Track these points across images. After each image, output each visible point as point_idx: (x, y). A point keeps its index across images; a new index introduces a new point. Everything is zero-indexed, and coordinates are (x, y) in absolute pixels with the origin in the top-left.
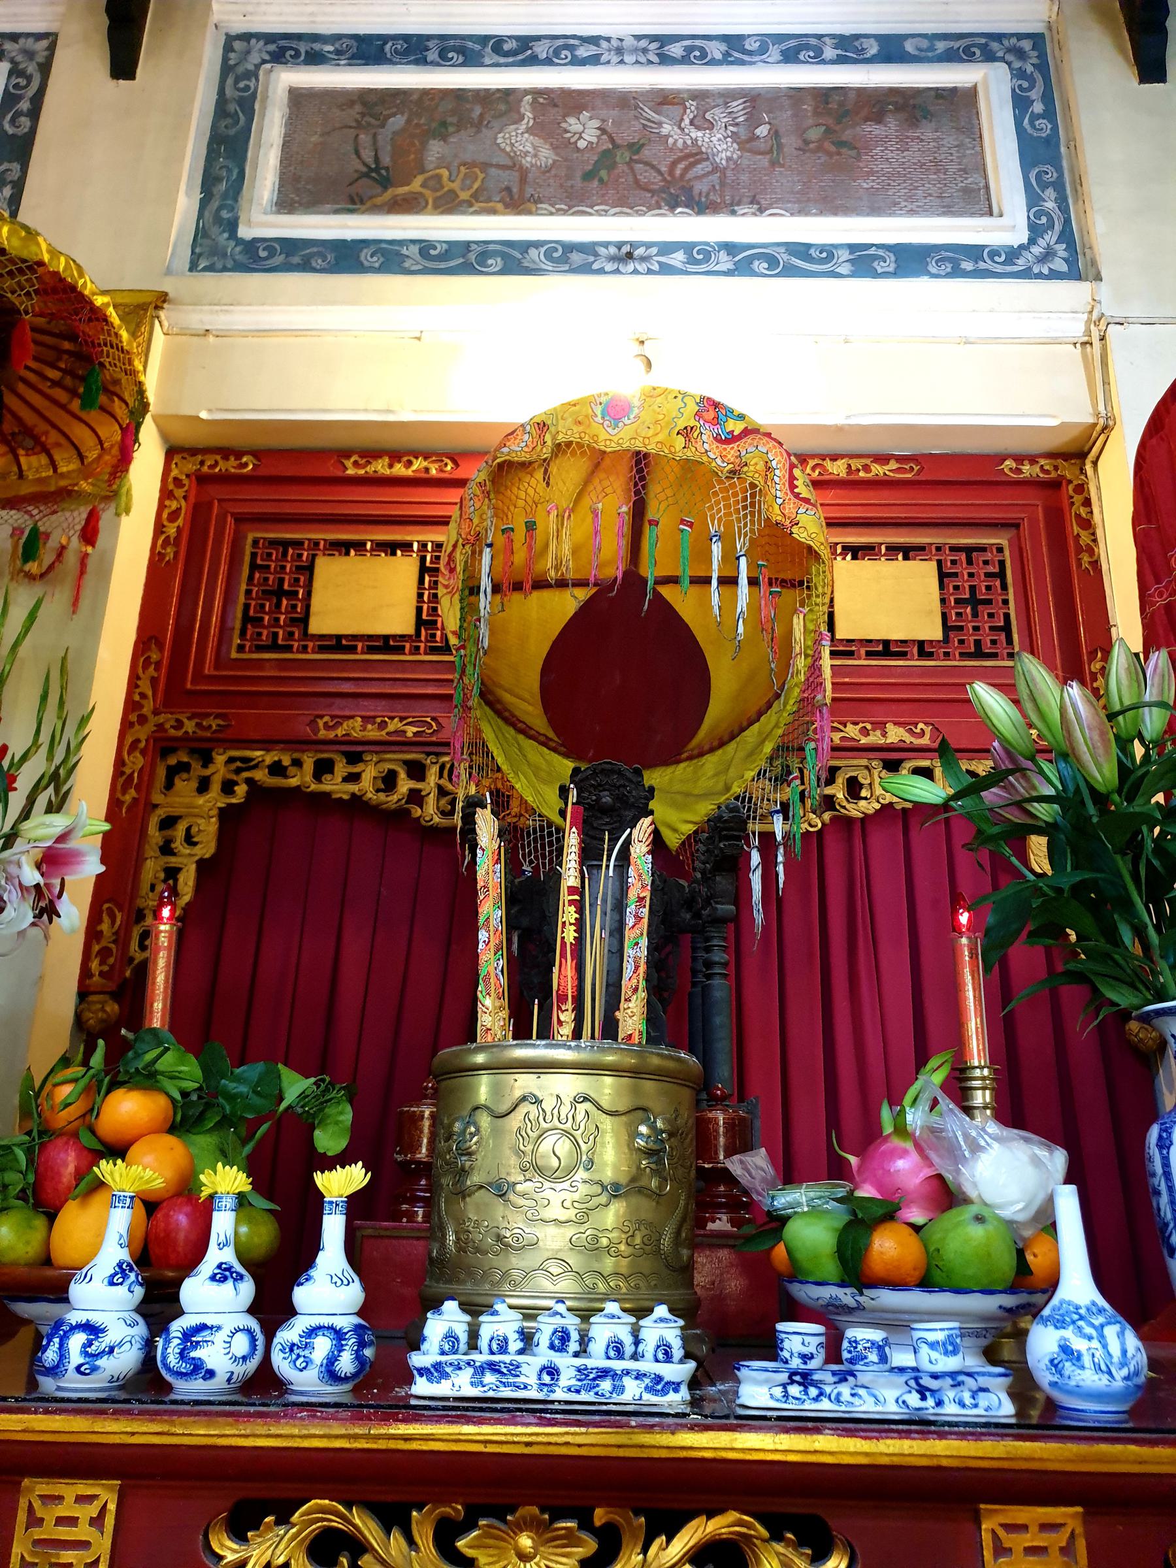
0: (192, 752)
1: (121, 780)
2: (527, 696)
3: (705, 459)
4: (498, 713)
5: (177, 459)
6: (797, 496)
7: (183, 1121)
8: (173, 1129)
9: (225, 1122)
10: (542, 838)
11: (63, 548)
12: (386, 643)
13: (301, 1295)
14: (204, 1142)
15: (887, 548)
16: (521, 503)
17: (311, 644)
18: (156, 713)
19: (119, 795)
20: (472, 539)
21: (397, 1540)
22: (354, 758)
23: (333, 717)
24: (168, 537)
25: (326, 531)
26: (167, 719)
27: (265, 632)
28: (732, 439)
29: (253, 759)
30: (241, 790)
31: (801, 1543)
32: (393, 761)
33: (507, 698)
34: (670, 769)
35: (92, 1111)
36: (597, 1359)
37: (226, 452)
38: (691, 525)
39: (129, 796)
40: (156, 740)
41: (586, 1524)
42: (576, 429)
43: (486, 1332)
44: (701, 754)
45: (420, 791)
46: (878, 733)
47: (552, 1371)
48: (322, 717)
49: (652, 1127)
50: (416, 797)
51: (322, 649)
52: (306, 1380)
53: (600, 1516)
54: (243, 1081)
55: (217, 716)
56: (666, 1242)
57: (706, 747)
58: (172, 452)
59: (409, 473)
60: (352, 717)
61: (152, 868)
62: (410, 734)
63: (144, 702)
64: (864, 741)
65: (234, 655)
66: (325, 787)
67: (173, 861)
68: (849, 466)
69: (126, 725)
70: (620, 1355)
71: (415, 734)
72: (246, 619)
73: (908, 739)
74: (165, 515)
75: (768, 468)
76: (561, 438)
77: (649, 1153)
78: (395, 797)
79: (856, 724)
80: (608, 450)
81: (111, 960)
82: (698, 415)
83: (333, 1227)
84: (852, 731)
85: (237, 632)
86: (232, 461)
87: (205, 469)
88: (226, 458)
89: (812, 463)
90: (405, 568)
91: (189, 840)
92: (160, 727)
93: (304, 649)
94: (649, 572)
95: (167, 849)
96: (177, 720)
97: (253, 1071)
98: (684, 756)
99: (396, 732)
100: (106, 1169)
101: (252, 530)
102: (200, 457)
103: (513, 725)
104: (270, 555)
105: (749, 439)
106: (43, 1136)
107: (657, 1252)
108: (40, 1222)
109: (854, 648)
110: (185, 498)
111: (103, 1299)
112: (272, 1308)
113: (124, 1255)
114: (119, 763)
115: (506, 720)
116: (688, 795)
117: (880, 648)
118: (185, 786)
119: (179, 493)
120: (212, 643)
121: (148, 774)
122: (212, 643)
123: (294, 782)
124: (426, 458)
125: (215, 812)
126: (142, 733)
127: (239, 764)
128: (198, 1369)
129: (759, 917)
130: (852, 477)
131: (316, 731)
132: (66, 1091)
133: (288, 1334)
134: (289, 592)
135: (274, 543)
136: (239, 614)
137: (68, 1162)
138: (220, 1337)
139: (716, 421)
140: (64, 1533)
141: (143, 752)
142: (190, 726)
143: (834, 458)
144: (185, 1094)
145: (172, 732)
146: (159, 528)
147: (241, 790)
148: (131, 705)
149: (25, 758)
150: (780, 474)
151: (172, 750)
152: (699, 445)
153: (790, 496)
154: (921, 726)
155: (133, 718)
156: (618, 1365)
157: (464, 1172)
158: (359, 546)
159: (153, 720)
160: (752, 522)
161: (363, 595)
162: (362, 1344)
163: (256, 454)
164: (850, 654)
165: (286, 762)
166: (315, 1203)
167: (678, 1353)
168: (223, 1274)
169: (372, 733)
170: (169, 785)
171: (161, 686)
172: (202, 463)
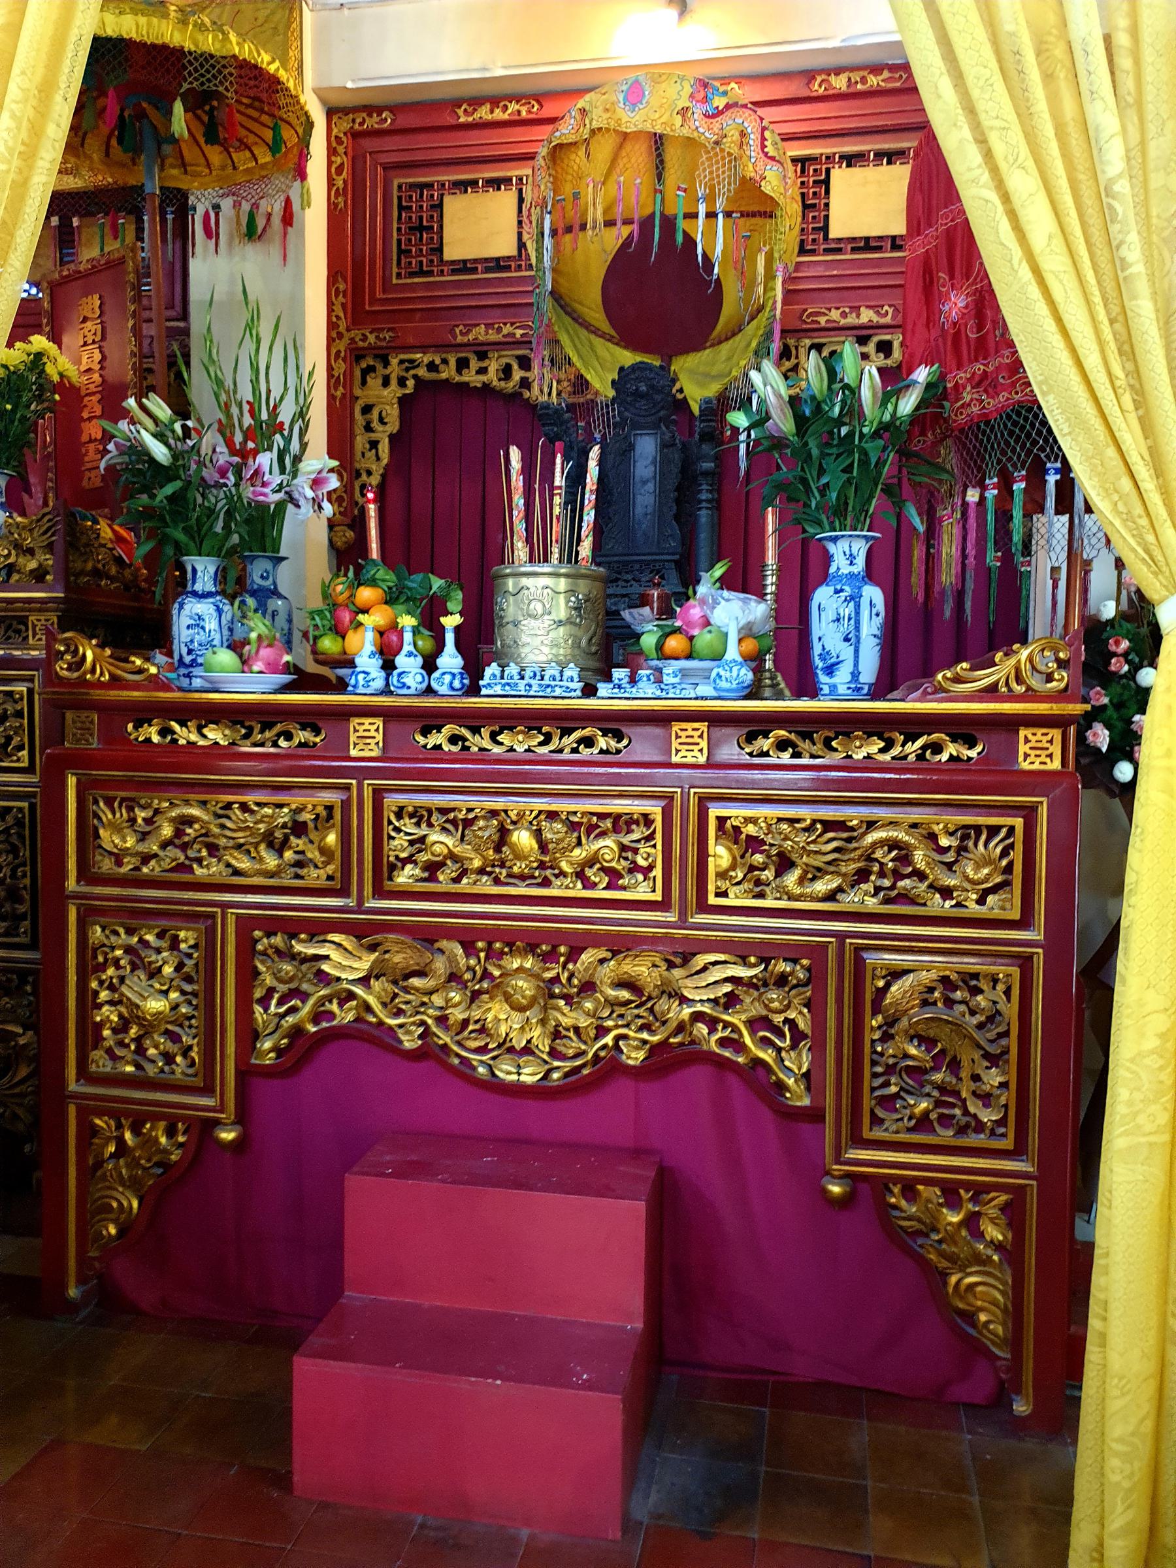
0: (376, 357)
1: (333, 381)
2: (593, 306)
3: (696, 134)
4: (575, 320)
7: (390, 599)
8: (386, 603)
9: (408, 599)
10: (608, 413)
11: (270, 215)
12: (499, 264)
13: (440, 662)
14: (400, 607)
15: (875, 155)
16: (569, 177)
17: (446, 269)
18: (348, 330)
19: (333, 391)
20: (540, 202)
21: (477, 736)
22: (482, 356)
23: (465, 326)
24: (338, 189)
26: (356, 334)
27: (414, 261)
28: (719, 113)
29: (414, 361)
30: (411, 383)
31: (614, 737)
32: (509, 357)
34: (700, 354)
35: (352, 596)
36: (546, 682)
37: (371, 109)
38: (685, 191)
40: (351, 350)
41: (540, 732)
42: (606, 116)
43: (506, 674)
44: (720, 342)
45: (527, 378)
46: (854, 315)
47: (530, 686)
48: (458, 326)
49: (577, 598)
50: (525, 383)
51: (454, 272)
52: (443, 690)
53: (545, 729)
54: (415, 581)
55: (389, 330)
56: (583, 643)
57: (723, 338)
59: (506, 117)
60: (478, 325)
61: (361, 442)
62: (518, 336)
63: (340, 323)
64: (843, 322)
65: (395, 281)
66: (465, 379)
67: (373, 436)
68: (850, 79)
70: (554, 680)
71: (522, 335)
72: (400, 252)
73: (875, 319)
74: (333, 170)
75: (743, 134)
76: (595, 125)
77: (575, 609)
78: (511, 384)
79: (837, 308)
80: (629, 131)
81: (344, 504)
82: (692, 96)
83: (450, 638)
84: (835, 315)
85: (395, 262)
87: (357, 126)
89: (819, 79)
90: (506, 199)
91: (382, 421)
92: (352, 339)
93: (442, 273)
95: (368, 428)
96: (363, 335)
97: (418, 577)
98: (708, 344)
99: (508, 335)
100: (361, 617)
101: (398, 176)
102: (351, 116)
103: (587, 328)
104: (411, 197)
106: (334, 607)
108: (340, 639)
109: (842, 245)
110: (345, 153)
111: (368, 662)
112: (429, 666)
113: (373, 649)
114: (330, 369)
115: (581, 324)
117: (862, 244)
118: (374, 382)
119: (341, 149)
120: (379, 273)
121: (349, 374)
122: (379, 273)
123: (444, 376)
124: (518, 102)
125: (395, 400)
126: (341, 345)
127: (407, 364)
128: (404, 685)
129: (743, 465)
130: (851, 90)
131: (455, 337)
132: (340, 588)
133: (436, 675)
134: (426, 228)
135: (412, 186)
137: (346, 617)
138: (411, 675)
139: (705, 100)
140: (366, 734)
141: (344, 360)
143: (838, 71)
144: (390, 588)
145: (361, 344)
146: (331, 182)
147: (411, 383)
148: (331, 326)
150: (754, 139)
151: (363, 357)
152: (691, 124)
153: (761, 155)
154: (886, 308)
155: (334, 335)
156: (553, 683)
157: (502, 617)
158: (473, 183)
159: (347, 336)
160: (729, 184)
161: (479, 226)
162: (462, 678)
163: (394, 109)
164: (839, 251)
165: (438, 361)
166: (442, 630)
167: (576, 679)
168: (410, 654)
169: (493, 336)
170: (364, 383)
171: (349, 311)
172: (354, 121)
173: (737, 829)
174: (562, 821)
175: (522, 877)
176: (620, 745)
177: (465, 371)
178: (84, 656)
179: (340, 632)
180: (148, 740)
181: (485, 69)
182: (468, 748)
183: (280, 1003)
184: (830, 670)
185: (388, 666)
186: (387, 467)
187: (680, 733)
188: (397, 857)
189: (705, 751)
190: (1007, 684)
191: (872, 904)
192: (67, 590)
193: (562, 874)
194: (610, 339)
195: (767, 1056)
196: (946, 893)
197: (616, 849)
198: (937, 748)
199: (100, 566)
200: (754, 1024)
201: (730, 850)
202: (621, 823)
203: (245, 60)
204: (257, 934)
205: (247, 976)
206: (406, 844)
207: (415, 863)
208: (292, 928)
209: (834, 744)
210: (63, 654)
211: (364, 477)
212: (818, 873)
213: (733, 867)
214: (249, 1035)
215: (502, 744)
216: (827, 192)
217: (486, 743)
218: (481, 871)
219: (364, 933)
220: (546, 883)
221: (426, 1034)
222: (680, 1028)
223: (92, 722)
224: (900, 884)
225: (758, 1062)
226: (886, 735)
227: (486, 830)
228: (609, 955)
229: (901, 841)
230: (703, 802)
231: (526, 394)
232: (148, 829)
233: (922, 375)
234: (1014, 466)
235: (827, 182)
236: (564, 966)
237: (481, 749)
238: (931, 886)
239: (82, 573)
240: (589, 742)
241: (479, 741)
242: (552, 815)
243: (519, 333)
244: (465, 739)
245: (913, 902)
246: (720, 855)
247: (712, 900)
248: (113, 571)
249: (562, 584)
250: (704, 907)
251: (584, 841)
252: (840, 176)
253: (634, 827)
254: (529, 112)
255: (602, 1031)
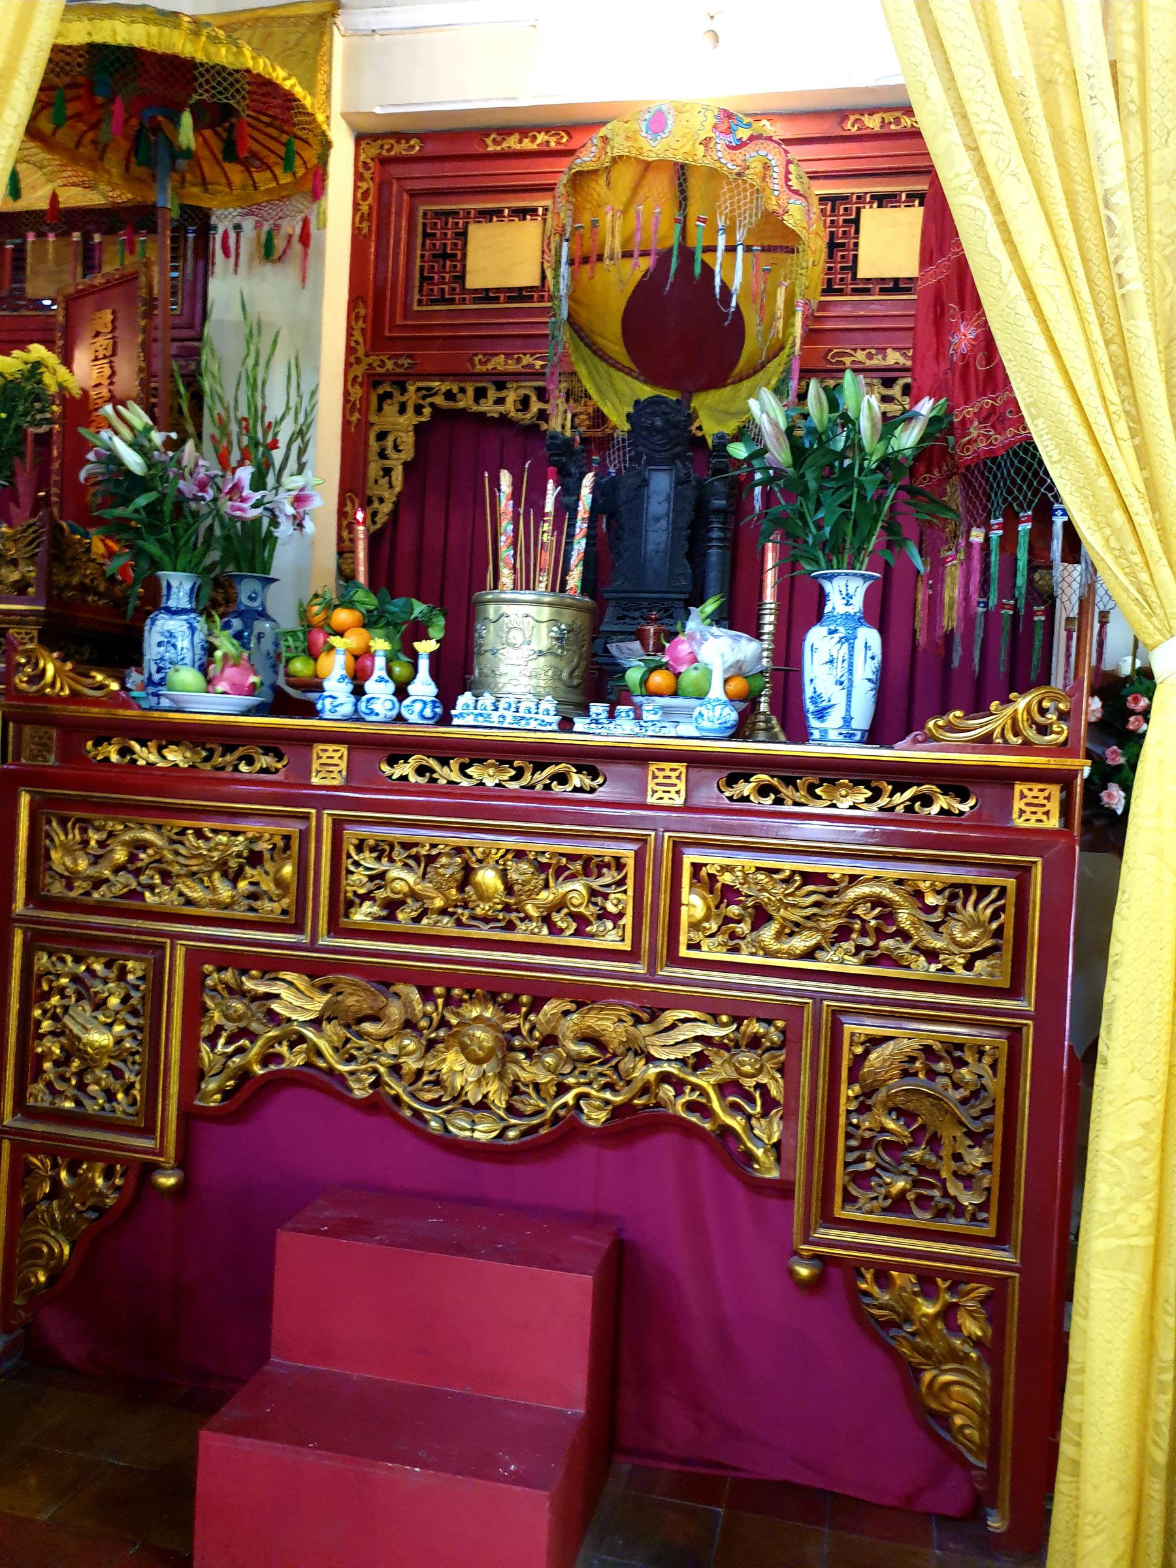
0: (394, 383)
4: (595, 352)
5: (363, 144)
6: (789, 187)
7: (369, 622)
8: (364, 626)
9: (388, 624)
11: (291, 236)
12: (520, 294)
13: (411, 689)
15: (908, 196)
18: (367, 355)
22: (501, 386)
25: (477, 202)
26: (374, 359)
28: (741, 145)
29: (431, 389)
30: (427, 411)
32: (527, 388)
33: (600, 340)
35: (328, 618)
36: (521, 714)
37: (399, 136)
39: (355, 417)
41: (512, 767)
44: (741, 380)
50: (543, 415)
51: (475, 301)
52: (413, 718)
53: (516, 763)
54: (396, 606)
55: (409, 356)
56: (564, 675)
58: (361, 138)
59: (534, 147)
61: (374, 469)
64: (869, 363)
65: (416, 308)
66: (483, 409)
67: (387, 463)
69: (348, 365)
72: (423, 279)
75: (766, 167)
76: (616, 153)
77: (557, 639)
78: (529, 416)
82: (715, 127)
83: (424, 664)
84: (860, 356)
85: (416, 290)
86: (404, 145)
87: (384, 152)
88: (398, 142)
89: (852, 118)
91: (396, 448)
94: (697, 240)
95: (382, 455)
102: (380, 142)
105: (752, 145)
106: (309, 627)
107: (560, 679)
111: (337, 688)
112: (401, 693)
113: (344, 672)
114: (346, 394)
116: (726, 413)
117: (891, 285)
118: (390, 408)
119: (367, 175)
121: (365, 399)
123: (461, 405)
126: (359, 371)
128: (372, 712)
130: (885, 131)
131: (474, 366)
132: (316, 609)
133: (407, 702)
134: (450, 256)
135: (438, 214)
136: (417, 275)
137: (320, 638)
139: (729, 131)
141: (361, 385)
142: (390, 365)
143: (871, 112)
144: (369, 611)
145: (379, 370)
146: (356, 206)
147: (427, 411)
148: (350, 350)
149: (283, 418)
150: (778, 172)
155: (352, 359)
157: (481, 645)
158: (499, 212)
159: (366, 361)
161: (505, 255)
163: (423, 137)
164: (866, 291)
165: (455, 390)
166: (414, 655)
167: (553, 712)
168: (381, 680)
169: (512, 367)
172: (382, 147)
173: (712, 878)
174: (530, 862)
175: (486, 920)
176: (595, 784)
177: (482, 401)
178: (44, 670)
179: (312, 654)
180: (107, 759)
181: (513, 99)
182: (434, 781)
183: (228, 1042)
184: (821, 714)
185: (358, 692)
186: (399, 496)
187: (657, 773)
188: (355, 893)
189: (683, 793)
190: (1003, 735)
191: (853, 967)
192: (48, 604)
193: (527, 918)
194: (629, 372)
195: (736, 1123)
196: (932, 955)
197: (584, 892)
198: (927, 800)
199: (87, 581)
200: (723, 1088)
201: (704, 899)
202: (591, 866)
203: (259, 75)
204: (208, 968)
205: (195, 1011)
206: (365, 879)
207: (373, 899)
208: (243, 964)
209: (818, 791)
210: (24, 665)
211: (376, 505)
212: (793, 929)
213: (707, 918)
214: (193, 1074)
215: (470, 777)
216: (857, 232)
217: (455, 776)
218: (443, 912)
219: (318, 972)
220: (510, 927)
221: (377, 1083)
222: (645, 1089)
223: (50, 738)
224: (883, 944)
225: (726, 1130)
226: (873, 784)
227: (449, 867)
228: (573, 1007)
229: (884, 898)
230: (678, 847)
231: (544, 426)
232: (100, 852)
233: (925, 407)
234: (1020, 506)
235: (856, 222)
236: (526, 1017)
237: (450, 782)
238: (915, 948)
239: (68, 586)
240: (562, 779)
241: (448, 774)
242: (520, 855)
243: (538, 364)
244: (433, 771)
245: (896, 963)
246: (694, 904)
247: (684, 952)
248: (102, 587)
249: (546, 613)
250: (674, 959)
251: (552, 883)
252: (871, 217)
253: (605, 870)
254: (558, 143)
255: (563, 1089)
